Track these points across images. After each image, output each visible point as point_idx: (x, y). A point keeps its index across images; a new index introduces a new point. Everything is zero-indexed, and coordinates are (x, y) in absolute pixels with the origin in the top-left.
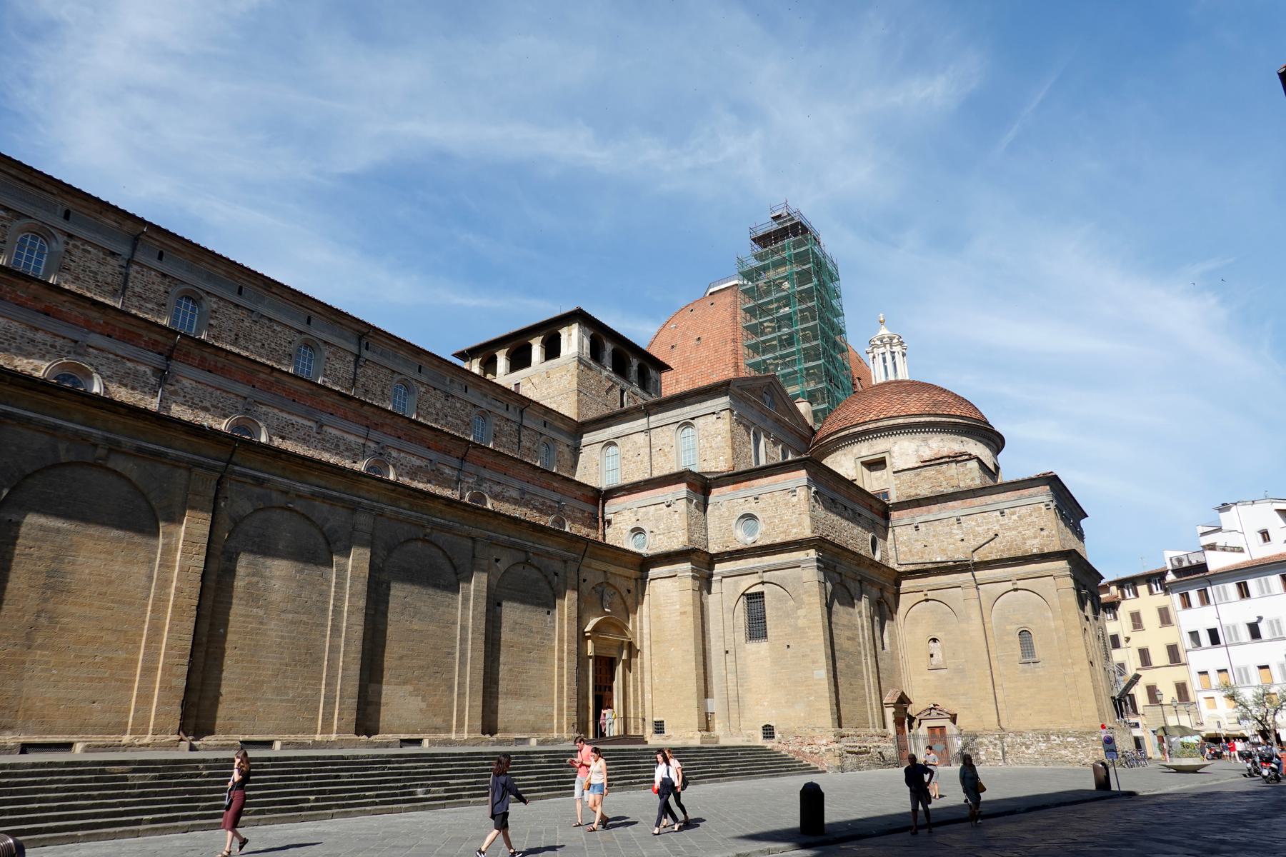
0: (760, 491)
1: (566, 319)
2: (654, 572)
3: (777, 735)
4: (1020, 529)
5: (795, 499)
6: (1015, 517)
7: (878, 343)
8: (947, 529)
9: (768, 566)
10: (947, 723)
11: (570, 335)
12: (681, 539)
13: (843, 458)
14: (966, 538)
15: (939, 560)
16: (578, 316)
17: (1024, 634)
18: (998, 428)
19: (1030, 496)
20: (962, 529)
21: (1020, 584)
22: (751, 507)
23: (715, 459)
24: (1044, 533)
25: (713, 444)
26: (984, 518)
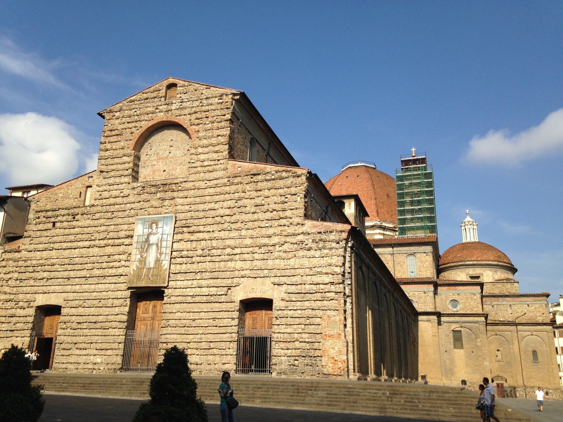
0: (461, 292)
1: (349, 197)
2: (420, 318)
3: (467, 383)
4: (535, 312)
5: (475, 297)
6: (533, 308)
7: (467, 223)
8: (505, 309)
9: (465, 321)
10: (504, 382)
11: (350, 204)
12: (431, 307)
13: (460, 274)
14: (513, 313)
15: (501, 320)
16: (356, 198)
17: (534, 353)
18: (515, 267)
19: (539, 300)
20: (511, 309)
21: (534, 333)
22: (456, 297)
23: (426, 271)
24: (544, 315)
25: (424, 265)
26: (521, 306)
